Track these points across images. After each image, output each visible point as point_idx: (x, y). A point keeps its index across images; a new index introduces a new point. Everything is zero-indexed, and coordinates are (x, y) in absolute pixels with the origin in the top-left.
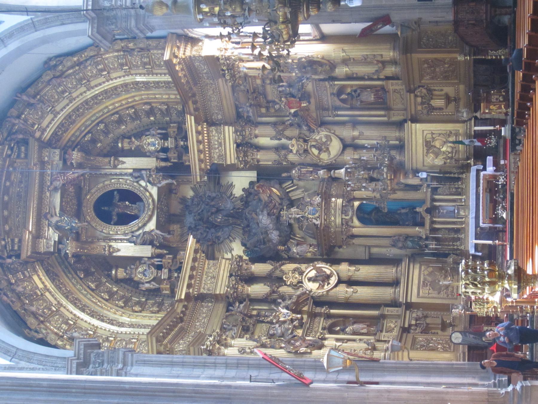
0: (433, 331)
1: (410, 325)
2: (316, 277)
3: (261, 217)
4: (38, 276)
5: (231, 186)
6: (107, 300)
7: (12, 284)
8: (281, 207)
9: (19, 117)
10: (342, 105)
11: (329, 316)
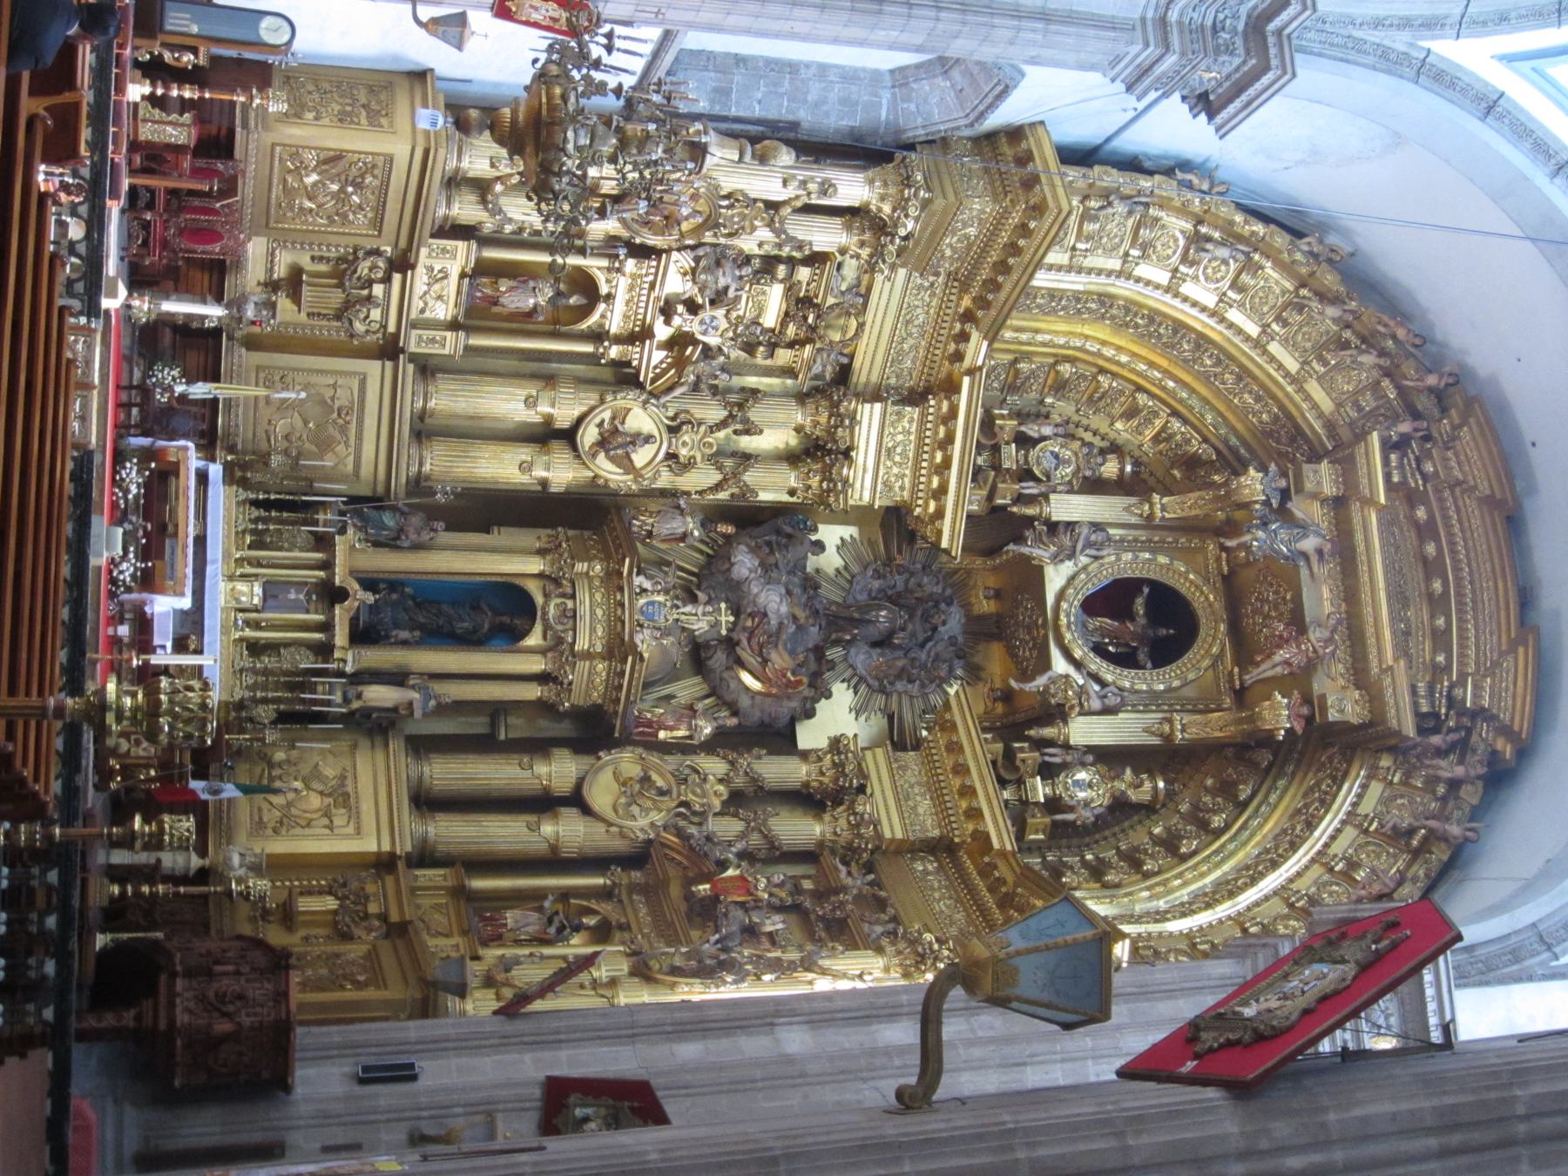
0: (323, 268)
1: (387, 280)
2: (633, 443)
3: (784, 609)
4: (1321, 415)
5: (858, 711)
6: (1139, 388)
7: (1387, 373)
8: (735, 636)
9: (1454, 785)
10: (594, 905)
11: (598, 336)
